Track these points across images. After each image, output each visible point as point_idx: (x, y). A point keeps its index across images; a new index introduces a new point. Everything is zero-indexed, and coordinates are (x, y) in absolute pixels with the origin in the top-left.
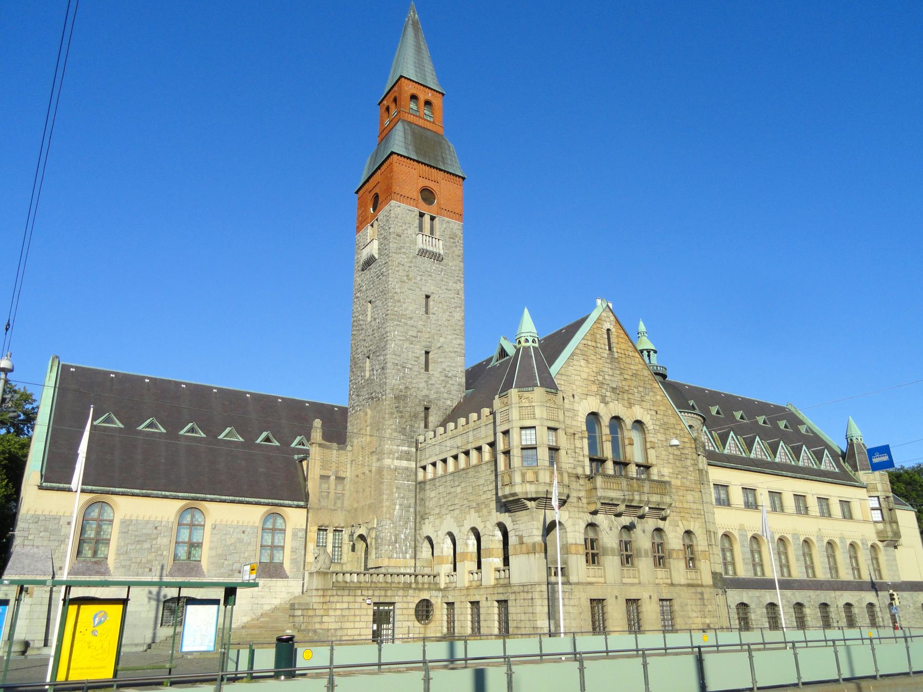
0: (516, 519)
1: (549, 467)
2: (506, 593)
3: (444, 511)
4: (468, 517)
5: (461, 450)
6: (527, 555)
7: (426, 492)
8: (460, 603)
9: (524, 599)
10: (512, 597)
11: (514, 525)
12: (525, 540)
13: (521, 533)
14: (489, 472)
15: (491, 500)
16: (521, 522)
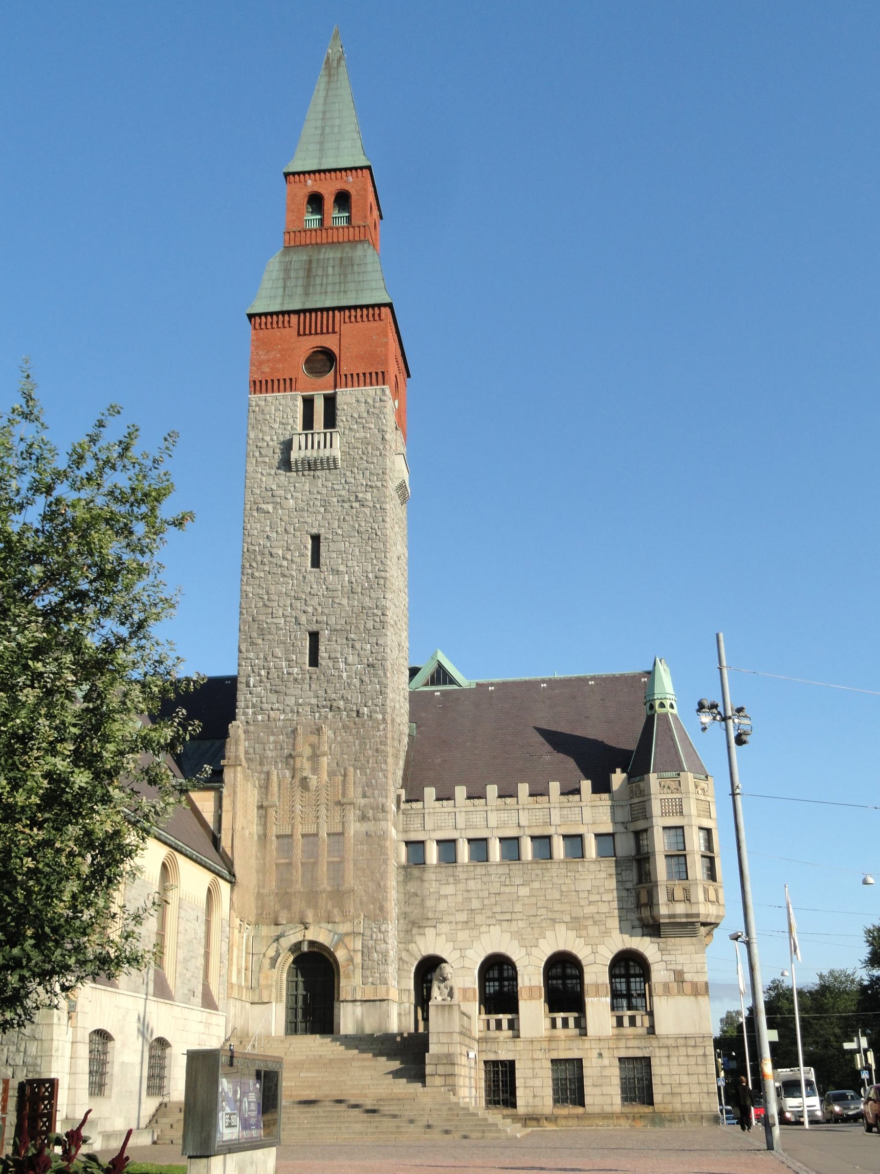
0: (669, 948)
1: (667, 880)
2: (645, 1047)
3: (479, 919)
4: (549, 934)
5: (529, 832)
6: (693, 998)
7: (426, 885)
8: (531, 1062)
9: (688, 1056)
10: (657, 1052)
11: (662, 955)
12: (688, 977)
13: (679, 967)
14: (603, 875)
15: (607, 915)
16: (680, 952)
